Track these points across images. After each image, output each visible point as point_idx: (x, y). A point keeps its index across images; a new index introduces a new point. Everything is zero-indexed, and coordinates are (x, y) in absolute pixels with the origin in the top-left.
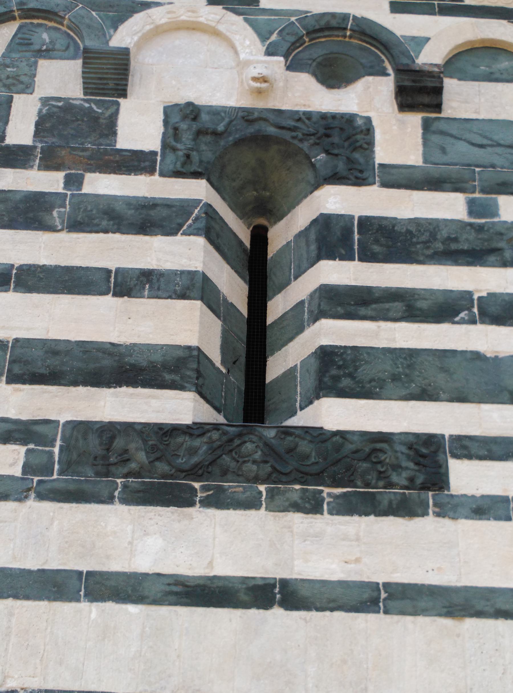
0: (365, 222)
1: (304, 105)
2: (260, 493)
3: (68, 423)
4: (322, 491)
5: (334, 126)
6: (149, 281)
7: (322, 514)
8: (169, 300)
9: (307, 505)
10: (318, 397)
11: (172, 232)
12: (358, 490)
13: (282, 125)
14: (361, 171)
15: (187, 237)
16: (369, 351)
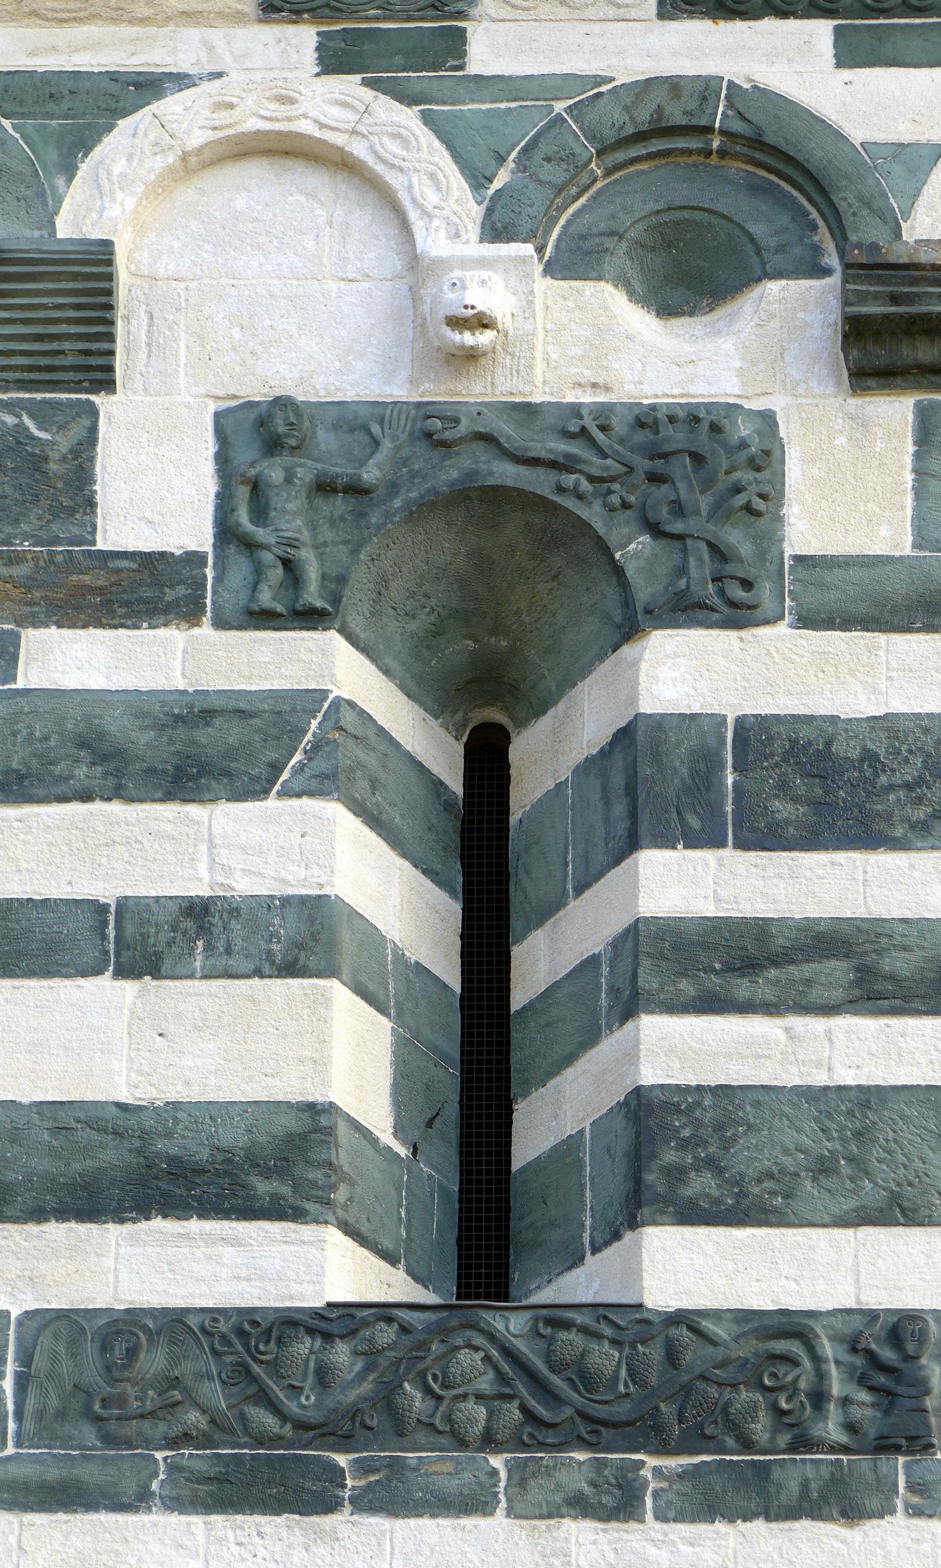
0: (754, 735)
1: (594, 385)
2: (494, 1472)
3: (29, 1315)
4: (643, 1463)
5: (674, 446)
6: (204, 930)
7: (642, 1521)
8: (256, 981)
9: (605, 1499)
10: (633, 1224)
11: (256, 789)
12: (728, 1458)
13: (533, 454)
14: (747, 584)
15: (295, 803)
16: (758, 1096)
